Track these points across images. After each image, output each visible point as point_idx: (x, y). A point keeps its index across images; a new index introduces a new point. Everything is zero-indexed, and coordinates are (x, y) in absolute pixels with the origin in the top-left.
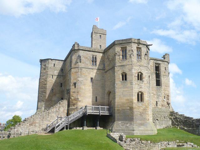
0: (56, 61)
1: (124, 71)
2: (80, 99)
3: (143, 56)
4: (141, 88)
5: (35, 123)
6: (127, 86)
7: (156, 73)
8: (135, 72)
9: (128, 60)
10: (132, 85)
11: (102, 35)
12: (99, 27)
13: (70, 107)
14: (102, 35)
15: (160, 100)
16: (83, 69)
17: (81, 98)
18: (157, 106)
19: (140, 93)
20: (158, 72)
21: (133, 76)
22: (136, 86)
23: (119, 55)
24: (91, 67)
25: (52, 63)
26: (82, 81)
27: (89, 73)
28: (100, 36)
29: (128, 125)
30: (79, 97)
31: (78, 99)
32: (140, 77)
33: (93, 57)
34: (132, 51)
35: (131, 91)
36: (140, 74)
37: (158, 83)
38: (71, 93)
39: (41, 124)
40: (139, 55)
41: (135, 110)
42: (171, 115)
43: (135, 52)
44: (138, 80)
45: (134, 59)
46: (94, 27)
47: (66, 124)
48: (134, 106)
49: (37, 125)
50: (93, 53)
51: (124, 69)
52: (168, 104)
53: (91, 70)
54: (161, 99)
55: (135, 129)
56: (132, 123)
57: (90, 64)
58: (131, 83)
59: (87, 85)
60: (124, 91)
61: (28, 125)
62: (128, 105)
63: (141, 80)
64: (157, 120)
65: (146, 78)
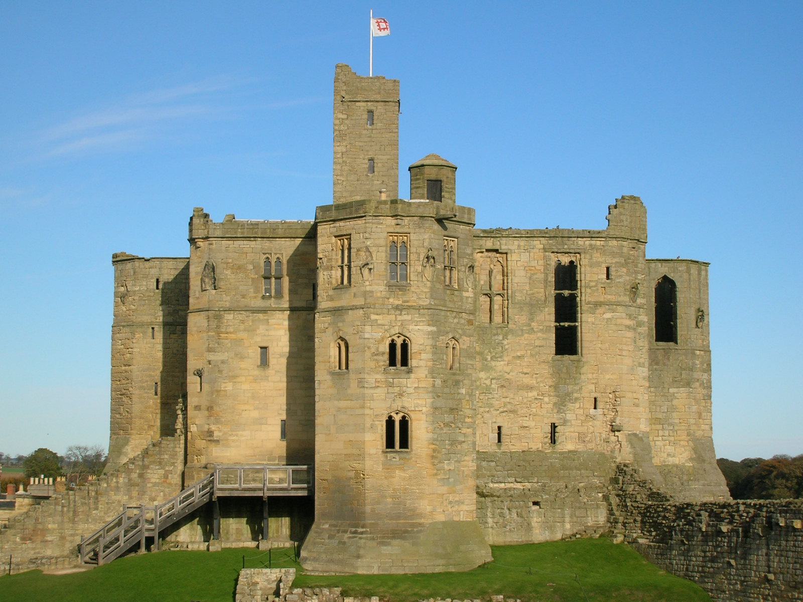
0: (165, 262)
1: (341, 334)
2: (216, 434)
3: (415, 266)
4: (401, 395)
5: (45, 531)
6: (349, 391)
7: (559, 299)
8: (375, 336)
9: (353, 290)
10: (362, 389)
11: (379, 109)
13: (189, 464)
14: (379, 109)
15: (569, 416)
16: (229, 317)
17: (220, 431)
18: (553, 441)
19: (397, 418)
20: (566, 293)
21: (368, 354)
22: (378, 390)
23: (330, 268)
24: (259, 303)
25: (146, 276)
26: (223, 362)
27: (251, 331)
28: (371, 112)
29: (347, 535)
30: (213, 428)
31: (210, 433)
32: (399, 355)
33: (268, 262)
34: (367, 249)
35: (360, 411)
36: (399, 342)
37: (567, 342)
38: (191, 412)
39: (68, 532)
41: (369, 483)
42: (615, 481)
43: (380, 258)
44: (392, 362)
45: (374, 284)
47: (147, 534)
48: (369, 464)
49: (49, 538)
50: (267, 244)
51: (340, 324)
53: (261, 316)
54: (574, 413)
55: (362, 552)
56: (360, 530)
57: (257, 291)
58: (361, 383)
59: (243, 379)
60: (339, 409)
61: (18, 539)
62: (351, 463)
63: (402, 365)
64: (535, 503)
65: (424, 356)
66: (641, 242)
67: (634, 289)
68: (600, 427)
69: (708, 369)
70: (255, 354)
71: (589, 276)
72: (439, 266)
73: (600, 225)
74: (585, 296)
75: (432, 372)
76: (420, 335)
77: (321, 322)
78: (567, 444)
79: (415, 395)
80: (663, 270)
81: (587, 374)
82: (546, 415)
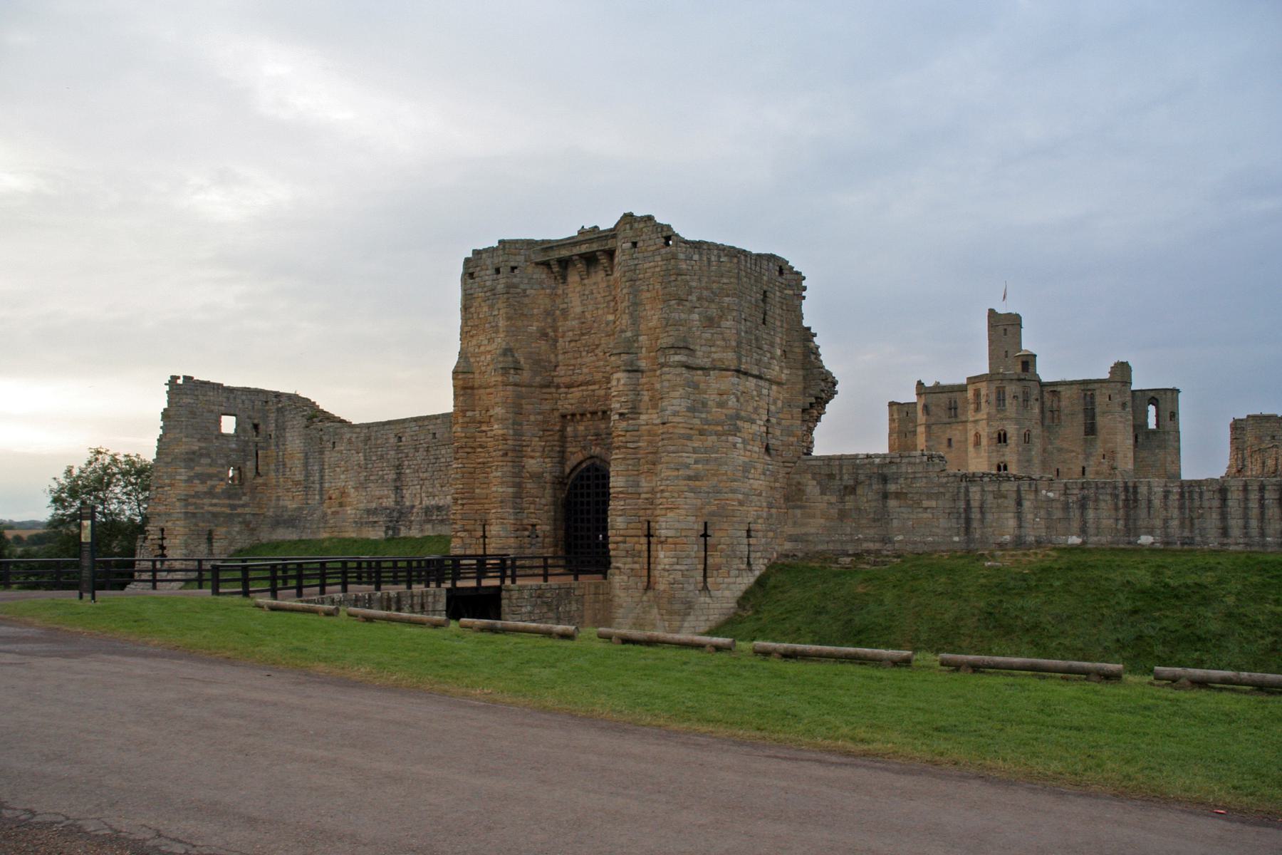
11: (1009, 328)
12: (1001, 310)
14: (1009, 328)
24: (946, 420)
32: (1002, 438)
40: (1001, 399)
43: (993, 397)
46: (992, 313)
52: (1114, 468)
66: (1128, 382)
67: (1124, 405)
68: (1105, 468)
69: (1178, 440)
70: (945, 442)
71: (1101, 400)
72: (1021, 400)
73: (1105, 375)
74: (1097, 410)
75: (1017, 445)
76: (1011, 430)
77: (970, 426)
78: (1090, 476)
79: (1010, 454)
80: (1152, 394)
81: (1099, 443)
82: (1080, 462)
